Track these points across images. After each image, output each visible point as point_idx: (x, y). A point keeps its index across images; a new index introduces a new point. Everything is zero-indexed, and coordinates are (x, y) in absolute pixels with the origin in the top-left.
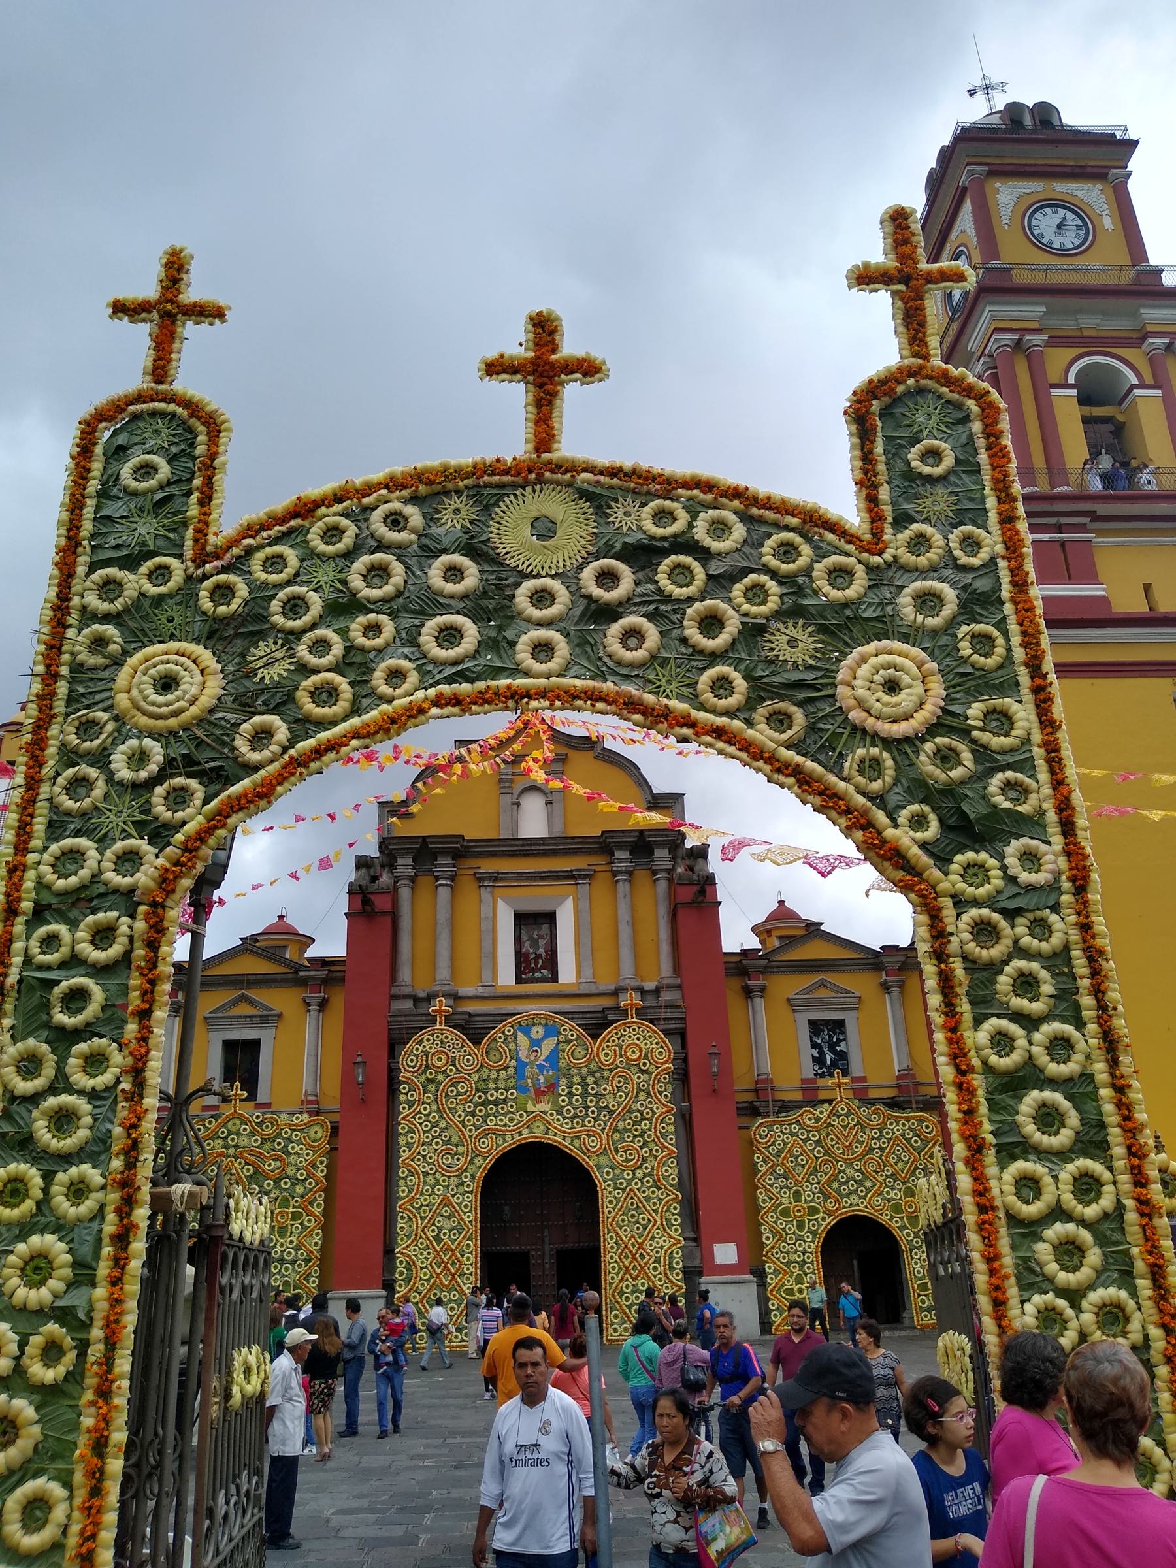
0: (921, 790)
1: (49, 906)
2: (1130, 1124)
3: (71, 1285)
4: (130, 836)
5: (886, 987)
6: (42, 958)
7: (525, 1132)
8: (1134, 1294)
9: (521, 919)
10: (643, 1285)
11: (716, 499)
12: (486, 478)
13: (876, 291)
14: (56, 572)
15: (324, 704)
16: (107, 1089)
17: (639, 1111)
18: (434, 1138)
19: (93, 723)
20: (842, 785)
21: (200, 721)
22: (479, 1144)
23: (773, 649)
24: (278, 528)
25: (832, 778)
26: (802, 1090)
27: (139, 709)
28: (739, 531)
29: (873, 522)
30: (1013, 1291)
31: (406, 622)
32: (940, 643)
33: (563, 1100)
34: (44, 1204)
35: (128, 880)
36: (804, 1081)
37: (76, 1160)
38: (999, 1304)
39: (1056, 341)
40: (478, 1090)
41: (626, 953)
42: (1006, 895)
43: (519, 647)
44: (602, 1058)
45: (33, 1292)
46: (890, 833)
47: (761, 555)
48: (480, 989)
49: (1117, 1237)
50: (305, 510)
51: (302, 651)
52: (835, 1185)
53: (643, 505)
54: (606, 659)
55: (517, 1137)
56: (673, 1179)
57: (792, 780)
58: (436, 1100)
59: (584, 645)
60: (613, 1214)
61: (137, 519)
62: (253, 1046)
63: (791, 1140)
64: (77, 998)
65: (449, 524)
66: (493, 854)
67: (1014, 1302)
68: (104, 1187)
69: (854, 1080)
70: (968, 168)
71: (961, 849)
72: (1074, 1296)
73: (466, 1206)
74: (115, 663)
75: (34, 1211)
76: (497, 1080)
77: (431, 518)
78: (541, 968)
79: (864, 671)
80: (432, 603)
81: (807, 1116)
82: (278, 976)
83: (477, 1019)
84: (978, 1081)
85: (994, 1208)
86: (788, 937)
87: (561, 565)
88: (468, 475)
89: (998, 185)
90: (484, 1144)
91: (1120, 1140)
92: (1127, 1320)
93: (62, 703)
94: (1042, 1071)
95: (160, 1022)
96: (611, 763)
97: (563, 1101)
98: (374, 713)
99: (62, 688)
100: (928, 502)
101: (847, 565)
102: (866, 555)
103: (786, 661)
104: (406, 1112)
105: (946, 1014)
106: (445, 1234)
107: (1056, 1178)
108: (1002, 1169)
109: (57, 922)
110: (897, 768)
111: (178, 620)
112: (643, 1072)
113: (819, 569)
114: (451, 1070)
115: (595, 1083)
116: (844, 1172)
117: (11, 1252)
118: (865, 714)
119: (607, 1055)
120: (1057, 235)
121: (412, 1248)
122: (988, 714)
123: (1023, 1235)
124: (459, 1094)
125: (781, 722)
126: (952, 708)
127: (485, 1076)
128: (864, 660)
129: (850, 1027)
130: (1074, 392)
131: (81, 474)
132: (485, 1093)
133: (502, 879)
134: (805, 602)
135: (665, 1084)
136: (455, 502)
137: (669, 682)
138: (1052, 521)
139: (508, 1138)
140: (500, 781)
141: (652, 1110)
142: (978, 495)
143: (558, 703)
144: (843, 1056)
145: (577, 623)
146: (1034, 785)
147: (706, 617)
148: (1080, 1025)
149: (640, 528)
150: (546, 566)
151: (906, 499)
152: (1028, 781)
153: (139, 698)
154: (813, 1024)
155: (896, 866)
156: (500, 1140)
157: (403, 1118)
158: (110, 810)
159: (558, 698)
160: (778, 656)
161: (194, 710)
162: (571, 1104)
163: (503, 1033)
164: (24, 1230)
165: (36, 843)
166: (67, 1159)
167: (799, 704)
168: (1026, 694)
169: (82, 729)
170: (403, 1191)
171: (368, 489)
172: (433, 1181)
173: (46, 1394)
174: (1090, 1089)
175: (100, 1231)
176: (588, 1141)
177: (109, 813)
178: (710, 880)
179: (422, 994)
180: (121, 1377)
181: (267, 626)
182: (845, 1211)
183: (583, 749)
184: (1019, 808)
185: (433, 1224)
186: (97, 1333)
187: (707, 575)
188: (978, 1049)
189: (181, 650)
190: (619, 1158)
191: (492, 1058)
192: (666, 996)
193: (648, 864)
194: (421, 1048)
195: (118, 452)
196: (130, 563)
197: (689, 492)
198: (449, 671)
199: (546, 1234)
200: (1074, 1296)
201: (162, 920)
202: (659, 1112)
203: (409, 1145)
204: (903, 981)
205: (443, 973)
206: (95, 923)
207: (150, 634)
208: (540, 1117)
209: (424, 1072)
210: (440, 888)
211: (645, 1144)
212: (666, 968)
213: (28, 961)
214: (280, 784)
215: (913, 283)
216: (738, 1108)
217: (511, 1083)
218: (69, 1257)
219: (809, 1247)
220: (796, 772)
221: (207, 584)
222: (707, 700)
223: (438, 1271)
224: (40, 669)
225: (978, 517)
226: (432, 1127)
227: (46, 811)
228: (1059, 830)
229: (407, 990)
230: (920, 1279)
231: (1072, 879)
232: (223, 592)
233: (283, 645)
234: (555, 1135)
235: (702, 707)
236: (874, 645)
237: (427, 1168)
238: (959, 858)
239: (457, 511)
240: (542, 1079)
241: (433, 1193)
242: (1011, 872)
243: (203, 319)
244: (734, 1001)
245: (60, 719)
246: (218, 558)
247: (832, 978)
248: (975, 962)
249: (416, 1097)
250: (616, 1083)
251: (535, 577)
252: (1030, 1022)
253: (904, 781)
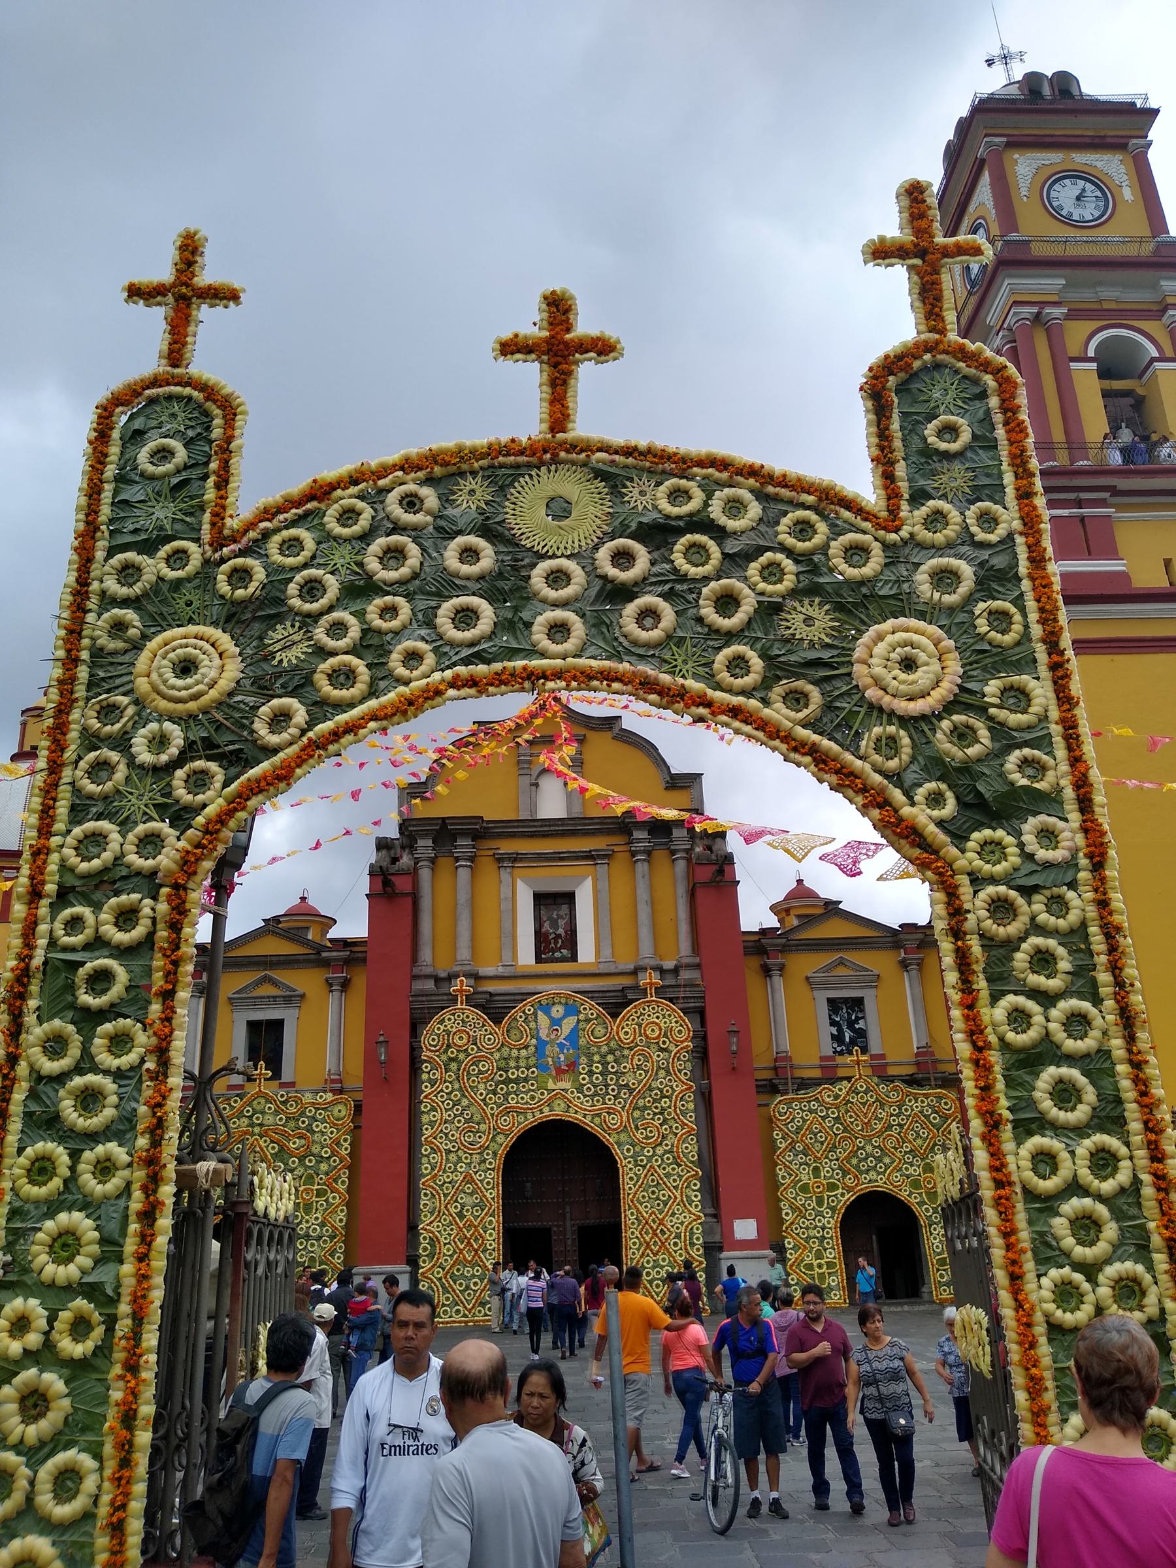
0: (938, 767)
1: (74, 887)
2: (1146, 1100)
3: (98, 1261)
4: (151, 819)
5: (904, 965)
6: (66, 939)
7: (546, 1110)
8: (1150, 1268)
9: (542, 900)
10: (664, 1260)
11: (731, 477)
12: (501, 458)
13: (892, 265)
14: (75, 557)
15: (342, 686)
16: (132, 1068)
19: (114, 707)
20: (859, 763)
21: (220, 704)
22: (501, 1122)
23: (789, 628)
24: (294, 511)
25: (848, 757)
26: (821, 1067)
27: (159, 693)
28: (755, 510)
29: (889, 499)
30: (1029, 1265)
31: (422, 604)
32: (957, 620)
33: (584, 1078)
34: (71, 1181)
35: (150, 862)
36: (822, 1059)
37: (102, 1139)
38: (1016, 1278)
39: (1075, 314)
40: (499, 1069)
41: (645, 933)
42: (1023, 872)
43: (535, 628)
44: (622, 1036)
45: (61, 1268)
46: (906, 811)
47: (777, 534)
49: (1134, 1211)
50: (321, 492)
51: (320, 633)
52: (854, 1161)
53: (658, 484)
54: (622, 639)
55: (538, 1115)
56: (693, 1156)
57: (808, 759)
58: (458, 1078)
59: (600, 625)
60: (634, 1190)
61: (155, 503)
62: (277, 1026)
63: (810, 1117)
64: (101, 979)
65: (465, 505)
66: (513, 835)
67: (1031, 1276)
68: (130, 1165)
69: (873, 1057)
70: (986, 139)
71: (978, 826)
72: (1090, 1270)
73: (488, 1183)
74: (135, 648)
75: (61, 1189)
76: (517, 1059)
77: (446, 500)
78: (561, 948)
79: (880, 649)
80: (448, 585)
81: (826, 1094)
82: (301, 957)
83: (497, 998)
84: (995, 1057)
85: (1011, 1184)
86: (807, 916)
87: (576, 545)
88: (483, 456)
89: (1016, 156)
90: (505, 1122)
91: (1137, 1115)
92: (1143, 1293)
93: (83, 687)
94: (1058, 1047)
95: (183, 1002)
96: (629, 743)
97: (584, 1079)
98: (392, 695)
99: (83, 673)
100: (945, 478)
101: (863, 542)
102: (882, 532)
103: (802, 639)
104: (428, 1091)
105: (963, 991)
106: (468, 1211)
107: (1072, 1153)
108: (1019, 1144)
109: (81, 904)
110: (914, 746)
111: (196, 604)
112: (662, 1050)
113: (836, 547)
115: (615, 1061)
116: (863, 1148)
117: (40, 1229)
118: (881, 692)
119: (626, 1033)
120: (1077, 206)
121: (435, 1224)
122: (1005, 691)
123: (1040, 1210)
124: (480, 1072)
125: (798, 701)
126: (969, 686)
128: (880, 638)
129: (869, 1006)
130: (1094, 366)
131: (98, 458)
132: (506, 1072)
133: (521, 860)
134: (822, 580)
136: (470, 483)
137: (685, 662)
138: (1071, 496)
139: (529, 1116)
140: (519, 762)
142: (995, 471)
143: (574, 684)
144: (862, 1034)
145: (592, 604)
146: (1051, 762)
147: (722, 597)
148: (1097, 1001)
149: (655, 507)
150: (562, 546)
151: (923, 476)
152: (1045, 758)
153: (158, 682)
154: (831, 1001)
155: (913, 844)
156: (521, 1118)
157: (426, 1097)
158: (131, 794)
159: (574, 678)
160: (794, 635)
161: (213, 693)
162: (591, 1082)
163: (524, 1012)
164: (52, 1207)
165: (59, 826)
166: (93, 1137)
167: (816, 683)
168: (1043, 670)
169: (103, 712)
170: (426, 1168)
171: (384, 471)
173: (76, 1369)
174: (1107, 1064)
175: (127, 1208)
177: (130, 797)
178: (728, 859)
179: (443, 975)
180: (149, 1351)
181: (285, 609)
182: (864, 1187)
183: (601, 730)
184: (1036, 785)
185: (456, 1201)
186: (124, 1308)
187: (723, 553)
188: (995, 1025)
189: (200, 634)
192: (685, 975)
193: (666, 844)
194: (442, 1028)
195: (135, 437)
196: (148, 547)
197: (705, 471)
198: (466, 652)
199: (568, 1210)
200: (1090, 1270)
201: (184, 902)
202: (678, 1089)
203: (432, 1123)
204: (922, 959)
205: (464, 953)
206: (119, 905)
207: (169, 618)
208: (561, 1095)
209: (446, 1051)
210: (460, 869)
211: (665, 1121)
212: (685, 947)
213: (53, 943)
214: (299, 766)
215: (929, 257)
216: (757, 1086)
217: (532, 1061)
218: (96, 1234)
219: (829, 1223)
220: (813, 751)
221: (225, 567)
222: (723, 679)
223: (462, 1247)
224: (61, 653)
225: (996, 492)
226: (454, 1105)
227: (68, 795)
228: (1076, 807)
229: (428, 971)
230: (939, 1254)
231: (1090, 856)
232: (241, 576)
233: (300, 628)
234: (576, 1112)
235: (718, 687)
236: (890, 623)
237: (450, 1146)
238: (976, 835)
239: (472, 492)
240: (562, 1057)
241: (456, 1170)
242: (1028, 849)
243: (218, 301)
244: (753, 980)
245: (81, 703)
246: (235, 541)
247: (850, 956)
248: (992, 939)
249: (438, 1075)
250: (635, 1061)
251: (550, 557)
252: (1047, 999)
253: (920, 759)
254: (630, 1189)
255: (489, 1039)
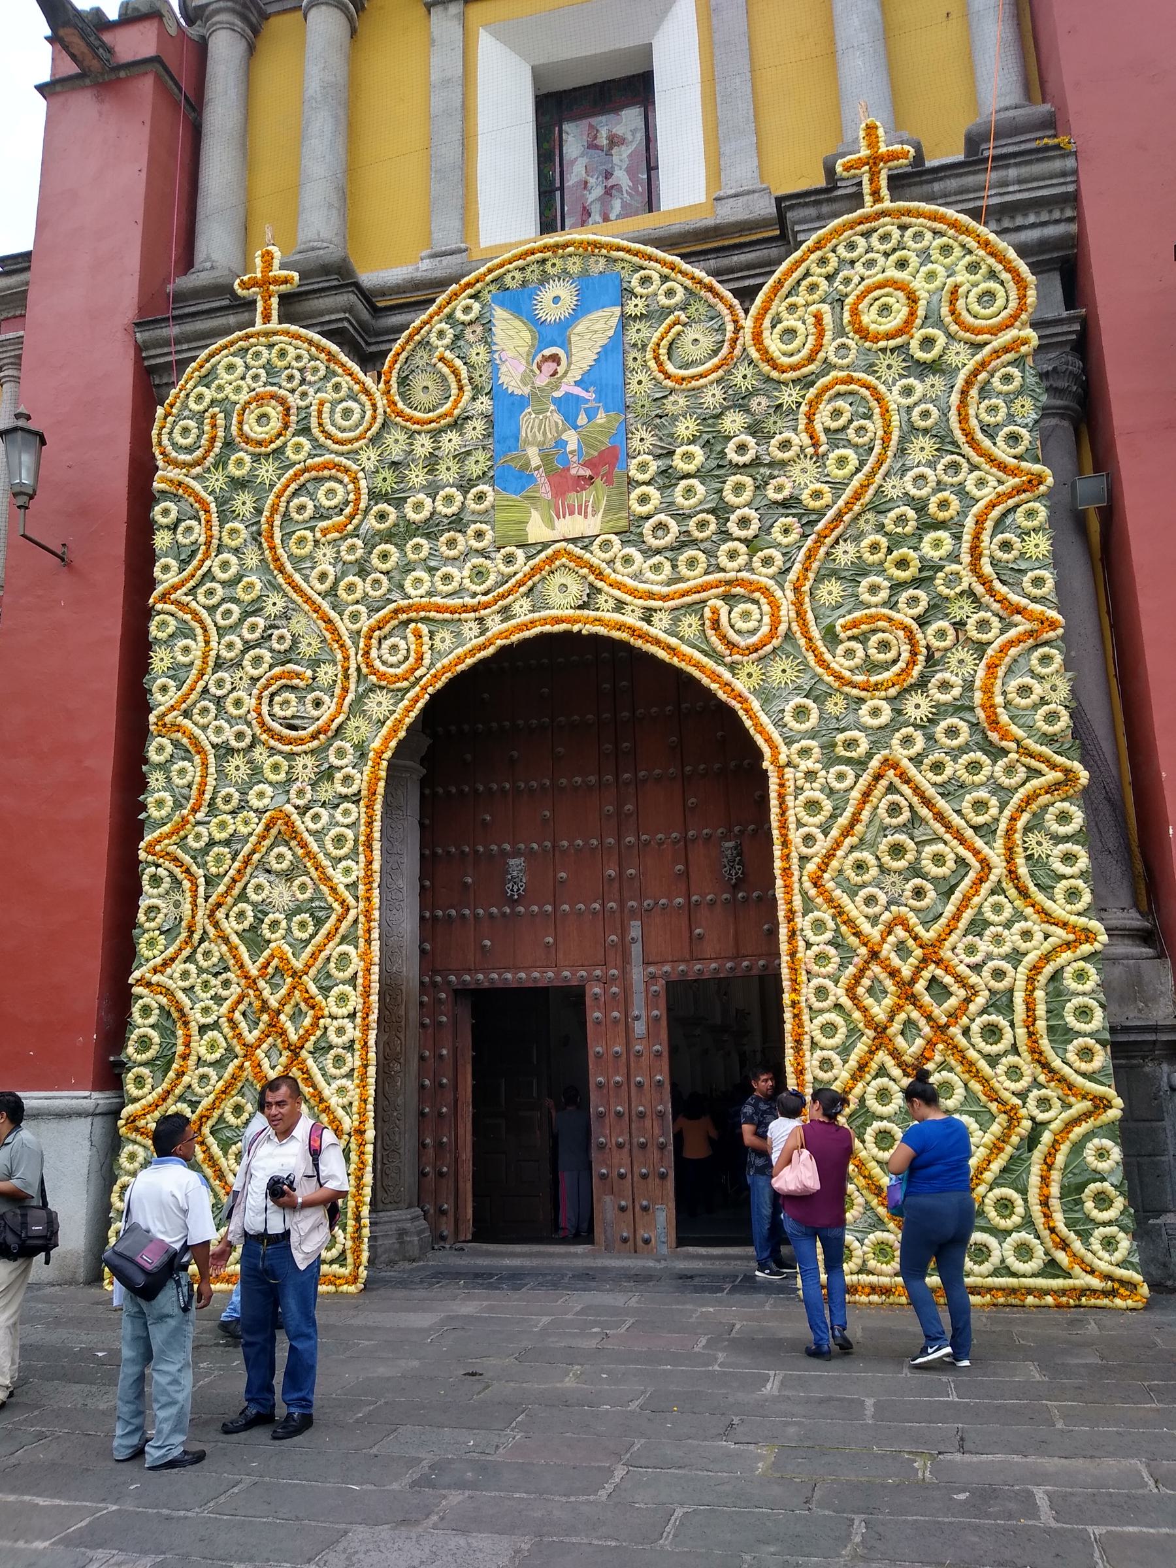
7: (522, 609)
17: (910, 500)
18: (248, 646)
44: (774, 344)
48: (425, 265)
55: (495, 626)
56: (1052, 717)
60: (822, 844)
73: (339, 840)
76: (432, 463)
97: (644, 500)
106: (274, 925)
112: (924, 369)
114: (298, 448)
115: (754, 429)
119: (791, 332)
121: (178, 967)
124: (321, 514)
127: (396, 452)
132: (399, 503)
135: (1009, 398)
139: (470, 630)
141: (960, 490)
157: (164, 598)
162: (668, 506)
170: (160, 803)
172: (245, 770)
176: (735, 619)
185: (243, 897)
190: (840, 663)
191: (419, 396)
194: (209, 394)
199: (635, 929)
202: (987, 494)
203: (177, 672)
211: (937, 606)
217: (474, 468)
223: (250, 1038)
226: (246, 615)
234: (620, 606)
237: (229, 734)
240: (572, 439)
249: (199, 533)
250: (823, 418)
254: (809, 839)
255: (347, 413)
